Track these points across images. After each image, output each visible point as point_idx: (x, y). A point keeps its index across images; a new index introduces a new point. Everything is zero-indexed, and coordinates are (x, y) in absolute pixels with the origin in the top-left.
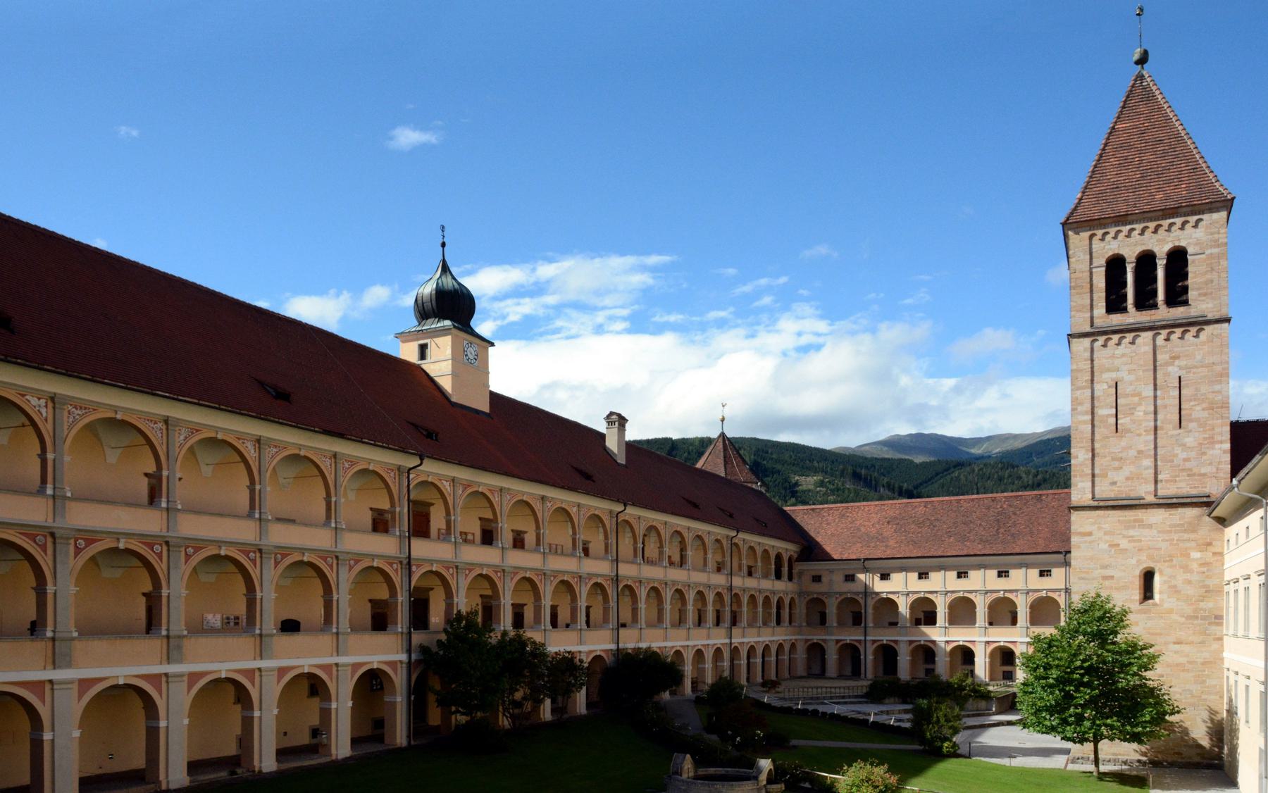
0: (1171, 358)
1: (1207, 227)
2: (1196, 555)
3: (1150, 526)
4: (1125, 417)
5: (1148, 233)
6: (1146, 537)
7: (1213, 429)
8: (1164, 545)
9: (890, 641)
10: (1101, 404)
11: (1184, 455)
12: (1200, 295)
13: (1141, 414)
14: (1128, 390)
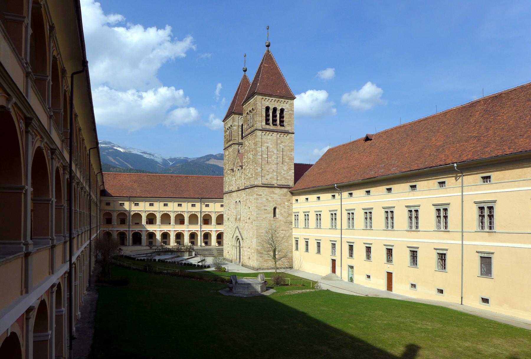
2: (286, 203)
3: (276, 194)
5: (275, 102)
7: (290, 166)
8: (279, 200)
11: (283, 173)
12: (288, 124)
13: (274, 158)
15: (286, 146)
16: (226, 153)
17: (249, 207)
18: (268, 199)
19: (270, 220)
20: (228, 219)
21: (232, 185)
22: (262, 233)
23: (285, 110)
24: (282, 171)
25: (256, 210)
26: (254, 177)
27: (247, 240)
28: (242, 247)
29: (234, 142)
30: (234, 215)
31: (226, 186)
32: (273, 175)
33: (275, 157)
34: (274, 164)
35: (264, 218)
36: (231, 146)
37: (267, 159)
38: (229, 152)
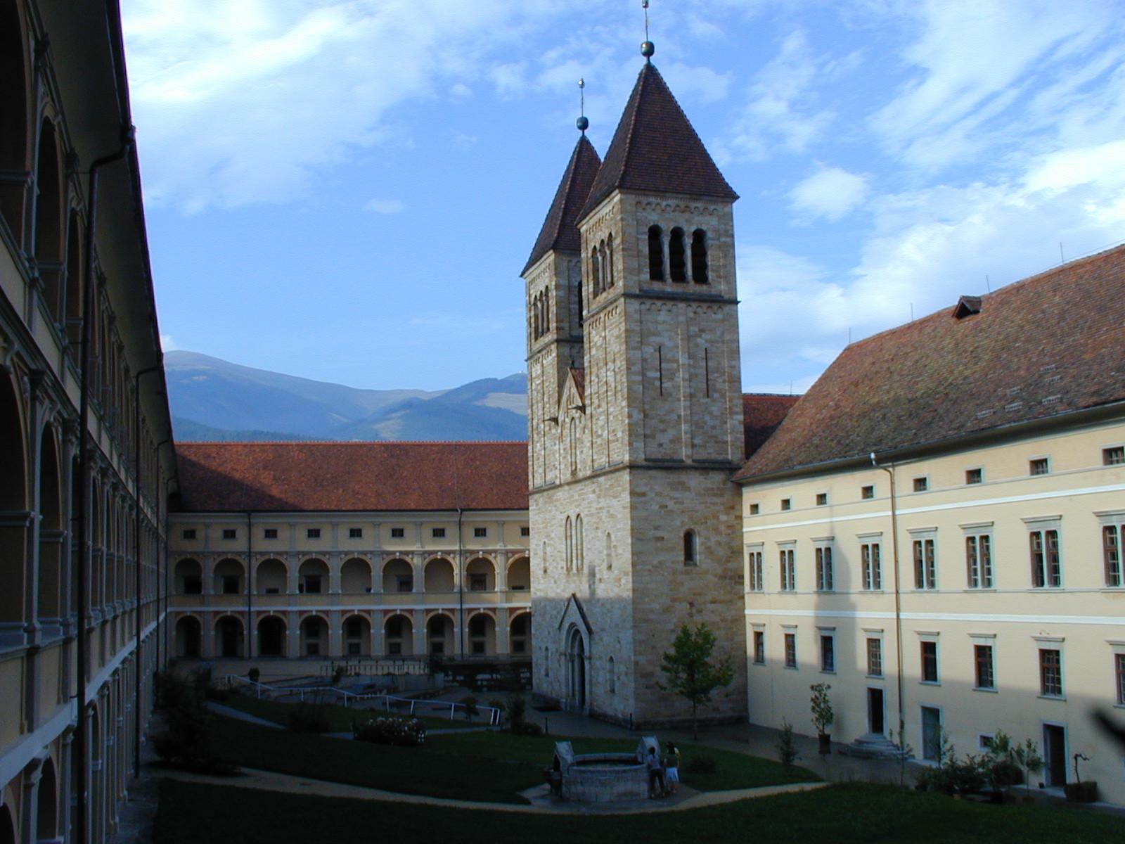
2: (723, 518)
3: (688, 489)
9: (446, 610)
11: (711, 423)
15: (716, 342)
18: (666, 506)
19: (675, 572)
20: (545, 571)
22: (652, 611)
23: (710, 234)
24: (707, 418)
26: (620, 440)
30: (562, 560)
35: (657, 567)
37: (658, 383)
38: (542, 365)
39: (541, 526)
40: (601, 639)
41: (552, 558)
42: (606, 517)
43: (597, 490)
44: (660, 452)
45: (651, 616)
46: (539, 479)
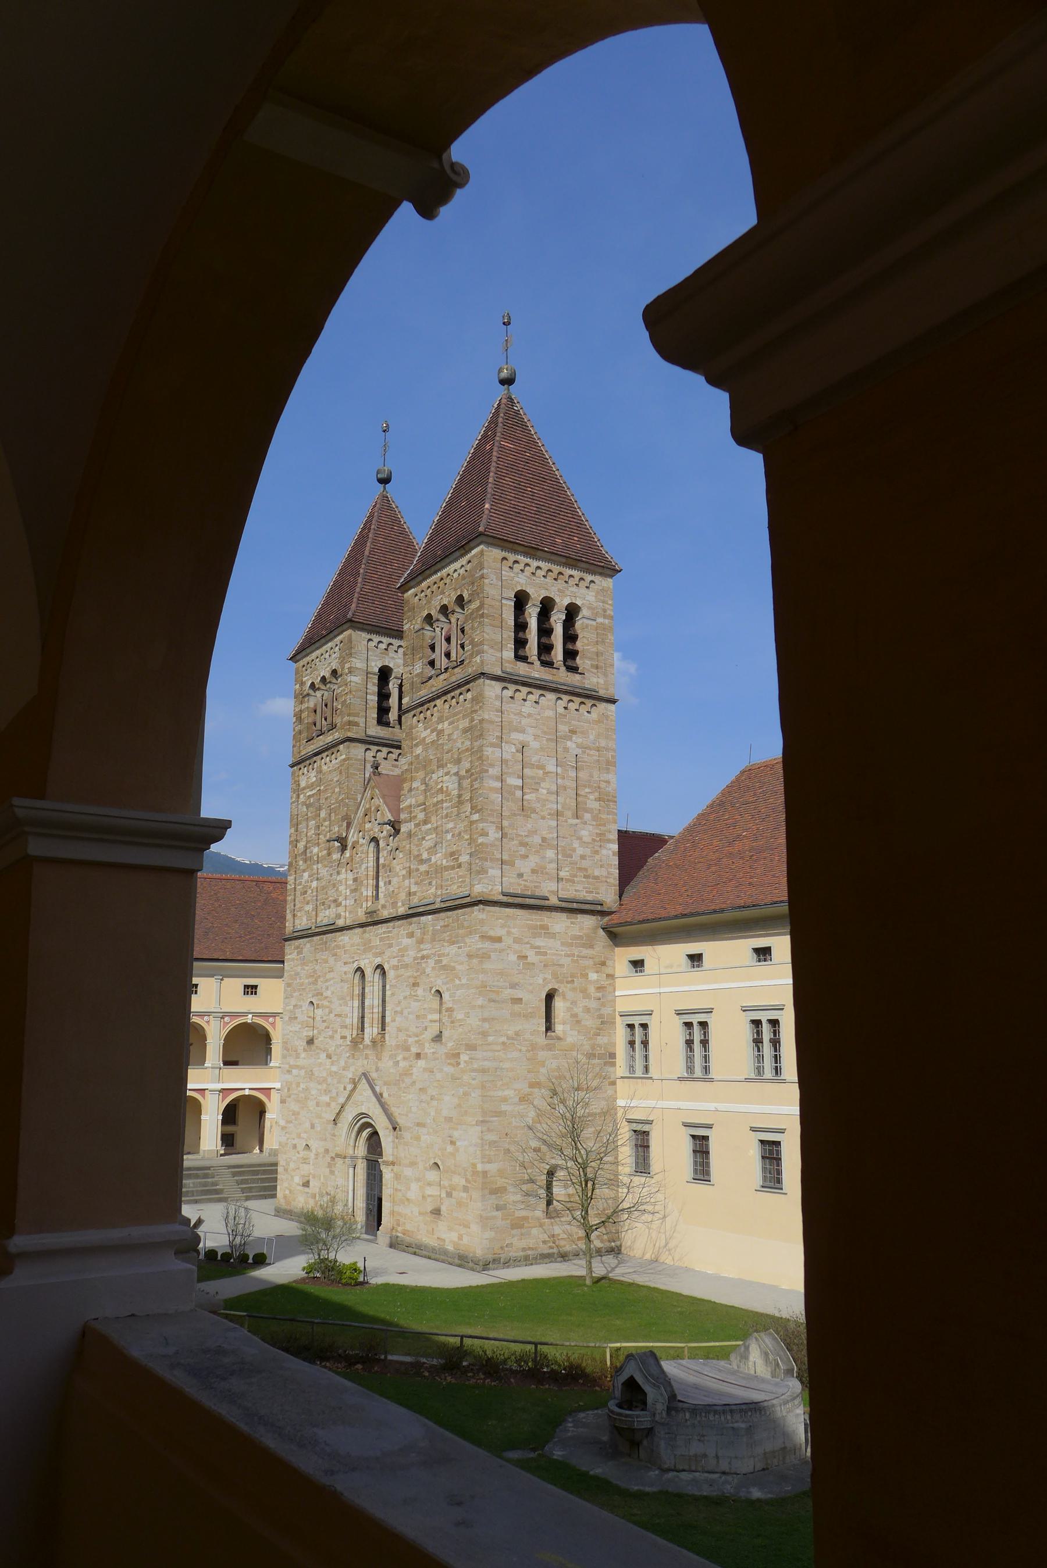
0: (570, 731)
1: (597, 593)
4: (530, 793)
6: (550, 948)
10: (510, 771)
14: (533, 761)
16: (302, 778)
17: (438, 991)
18: (526, 957)
19: (533, 1047)
20: (310, 1042)
21: (335, 901)
22: (504, 1100)
25: (480, 1001)
27: (424, 1130)
28: (393, 1164)
29: (350, 734)
31: (301, 909)
32: (544, 857)
33: (548, 789)
34: (545, 813)
35: (513, 1039)
36: (335, 750)
37: (519, 793)
38: (320, 771)
39: (307, 981)
40: (418, 1138)
41: (325, 1024)
42: (433, 968)
43: (418, 933)
44: (519, 885)
45: (504, 1107)
46: (305, 919)
